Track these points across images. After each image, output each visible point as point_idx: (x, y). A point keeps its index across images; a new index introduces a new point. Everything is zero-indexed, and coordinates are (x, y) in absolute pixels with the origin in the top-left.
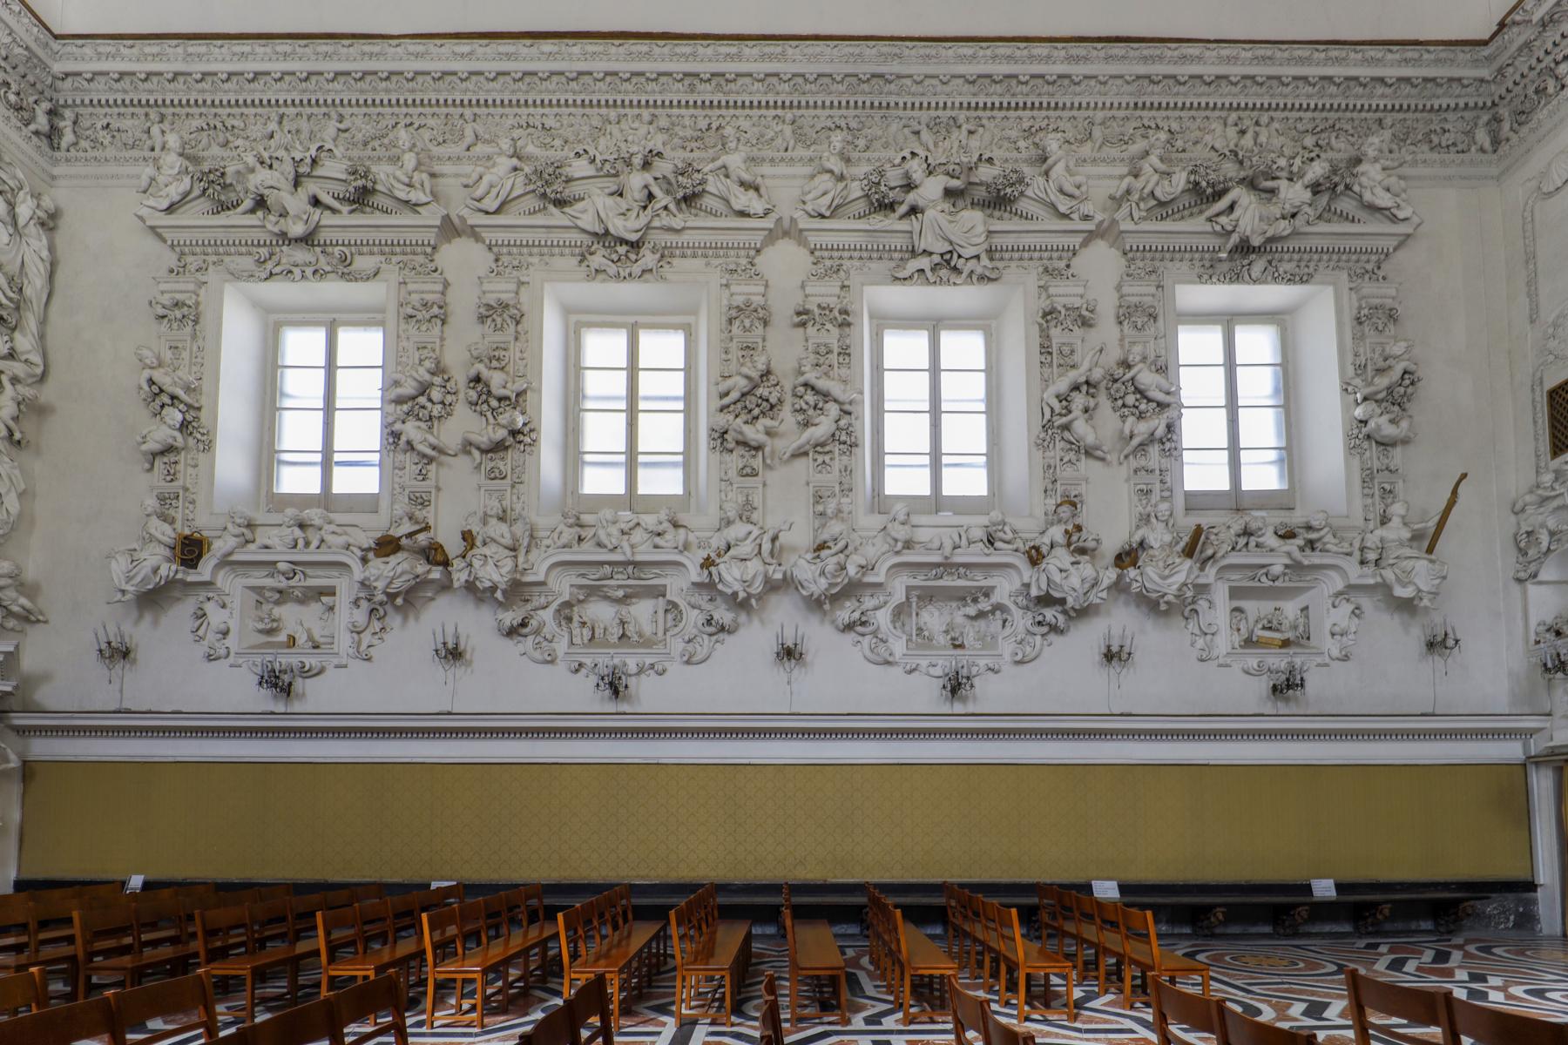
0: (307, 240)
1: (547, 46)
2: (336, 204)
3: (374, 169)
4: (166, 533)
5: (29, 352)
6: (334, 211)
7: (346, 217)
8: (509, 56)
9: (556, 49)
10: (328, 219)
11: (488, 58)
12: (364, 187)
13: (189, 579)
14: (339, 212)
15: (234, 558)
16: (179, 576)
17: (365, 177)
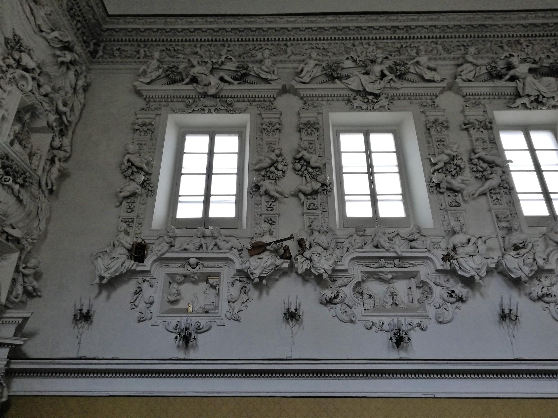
0: (214, 96)
1: (330, 18)
2: (232, 81)
3: (250, 66)
4: (128, 241)
5: (67, 146)
6: (230, 83)
7: (236, 86)
8: (312, 22)
9: (334, 18)
10: (227, 87)
11: (302, 23)
12: (246, 73)
13: (138, 269)
14: (233, 84)
15: (166, 256)
16: (134, 267)
17: (247, 69)
